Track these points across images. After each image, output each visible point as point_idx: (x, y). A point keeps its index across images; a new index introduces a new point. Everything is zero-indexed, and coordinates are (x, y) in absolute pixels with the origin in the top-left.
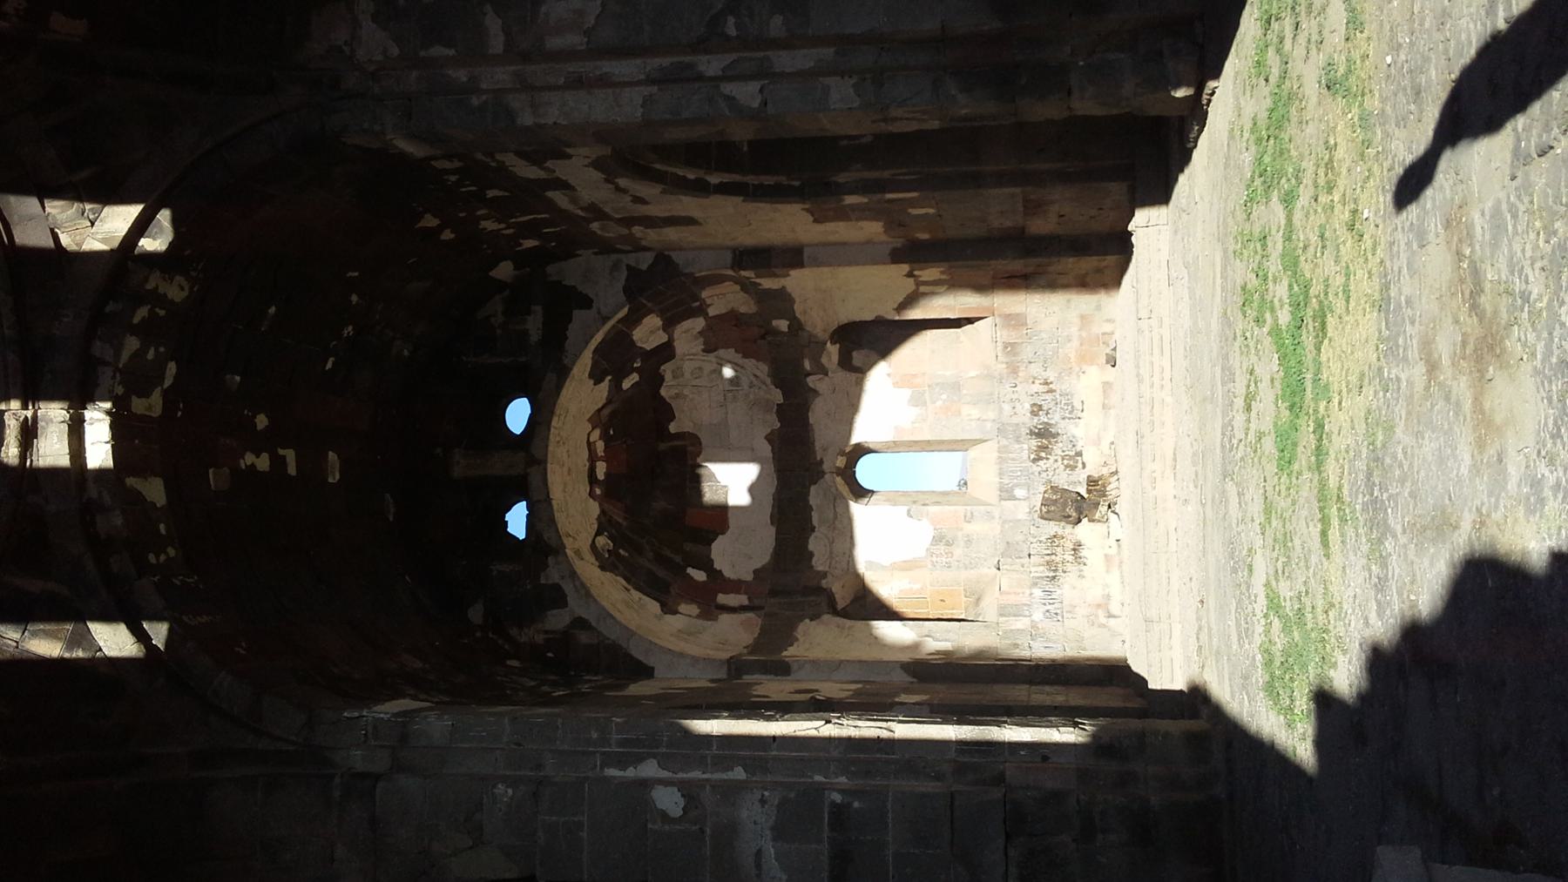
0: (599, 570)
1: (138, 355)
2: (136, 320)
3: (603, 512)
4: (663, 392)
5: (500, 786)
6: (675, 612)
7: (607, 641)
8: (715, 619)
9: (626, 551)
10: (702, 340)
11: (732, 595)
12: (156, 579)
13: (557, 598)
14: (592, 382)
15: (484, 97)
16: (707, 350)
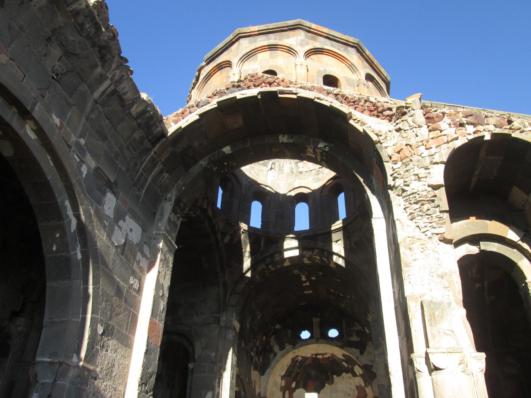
0: (291, 358)
1: (316, 259)
2: (323, 258)
3: (308, 358)
4: (344, 374)
5: (215, 353)
6: (282, 379)
7: (271, 362)
8: (281, 391)
9: (298, 365)
10: (359, 385)
11: (288, 395)
12: (265, 268)
13: (282, 348)
14: (342, 354)
15: (381, 341)
16: (357, 387)
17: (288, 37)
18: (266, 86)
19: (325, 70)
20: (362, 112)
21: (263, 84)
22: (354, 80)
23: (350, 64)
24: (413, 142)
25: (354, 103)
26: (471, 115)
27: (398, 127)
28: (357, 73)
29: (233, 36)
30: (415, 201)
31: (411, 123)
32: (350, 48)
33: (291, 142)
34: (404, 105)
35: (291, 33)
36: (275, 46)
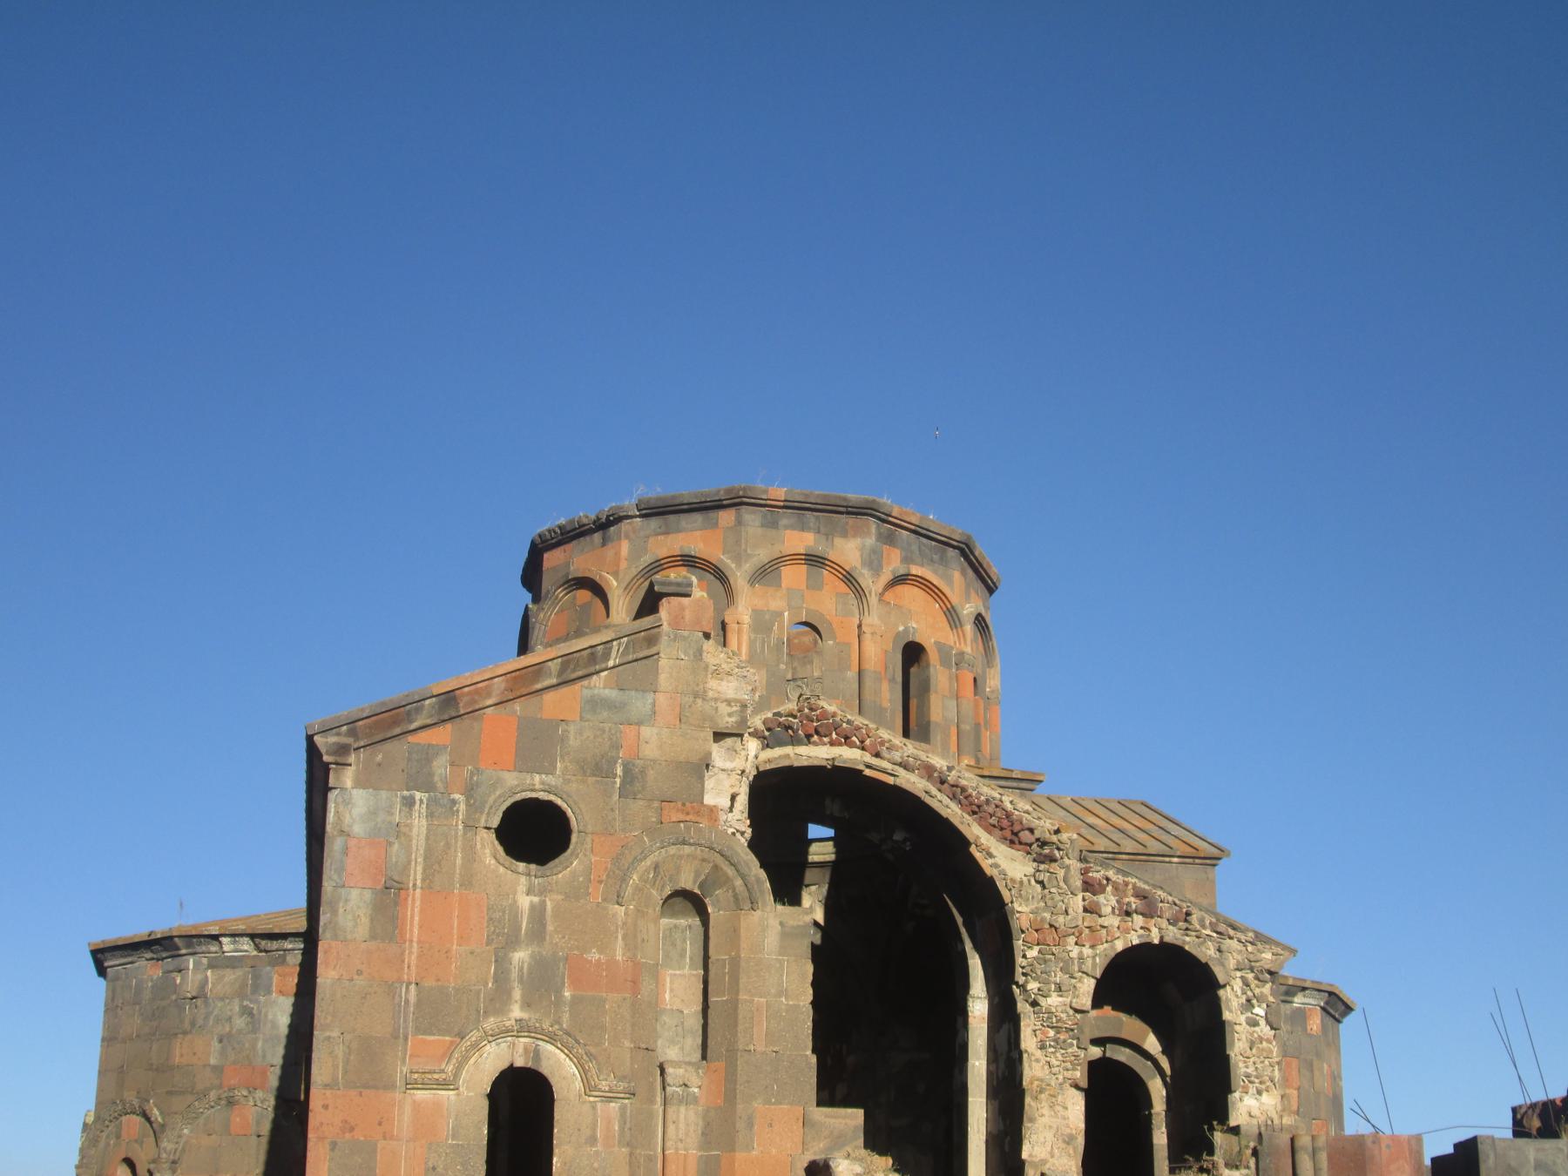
17: (845, 535)
18: (840, 744)
19: (906, 630)
20: (990, 833)
21: (834, 736)
22: (952, 648)
23: (949, 606)
24: (1061, 920)
25: (976, 809)
26: (1145, 898)
27: (1041, 877)
28: (959, 630)
29: (728, 491)
30: (1051, 1025)
31: (1062, 884)
32: (951, 553)
33: (847, 817)
34: (1054, 838)
35: (851, 520)
36: (821, 560)
